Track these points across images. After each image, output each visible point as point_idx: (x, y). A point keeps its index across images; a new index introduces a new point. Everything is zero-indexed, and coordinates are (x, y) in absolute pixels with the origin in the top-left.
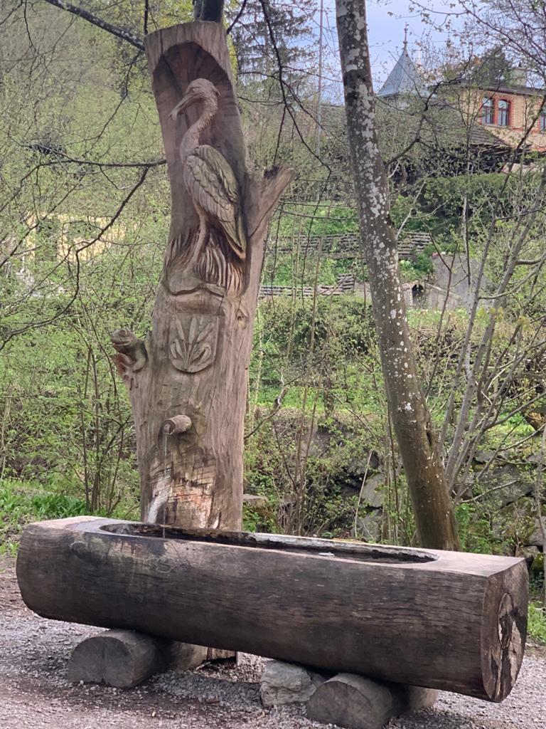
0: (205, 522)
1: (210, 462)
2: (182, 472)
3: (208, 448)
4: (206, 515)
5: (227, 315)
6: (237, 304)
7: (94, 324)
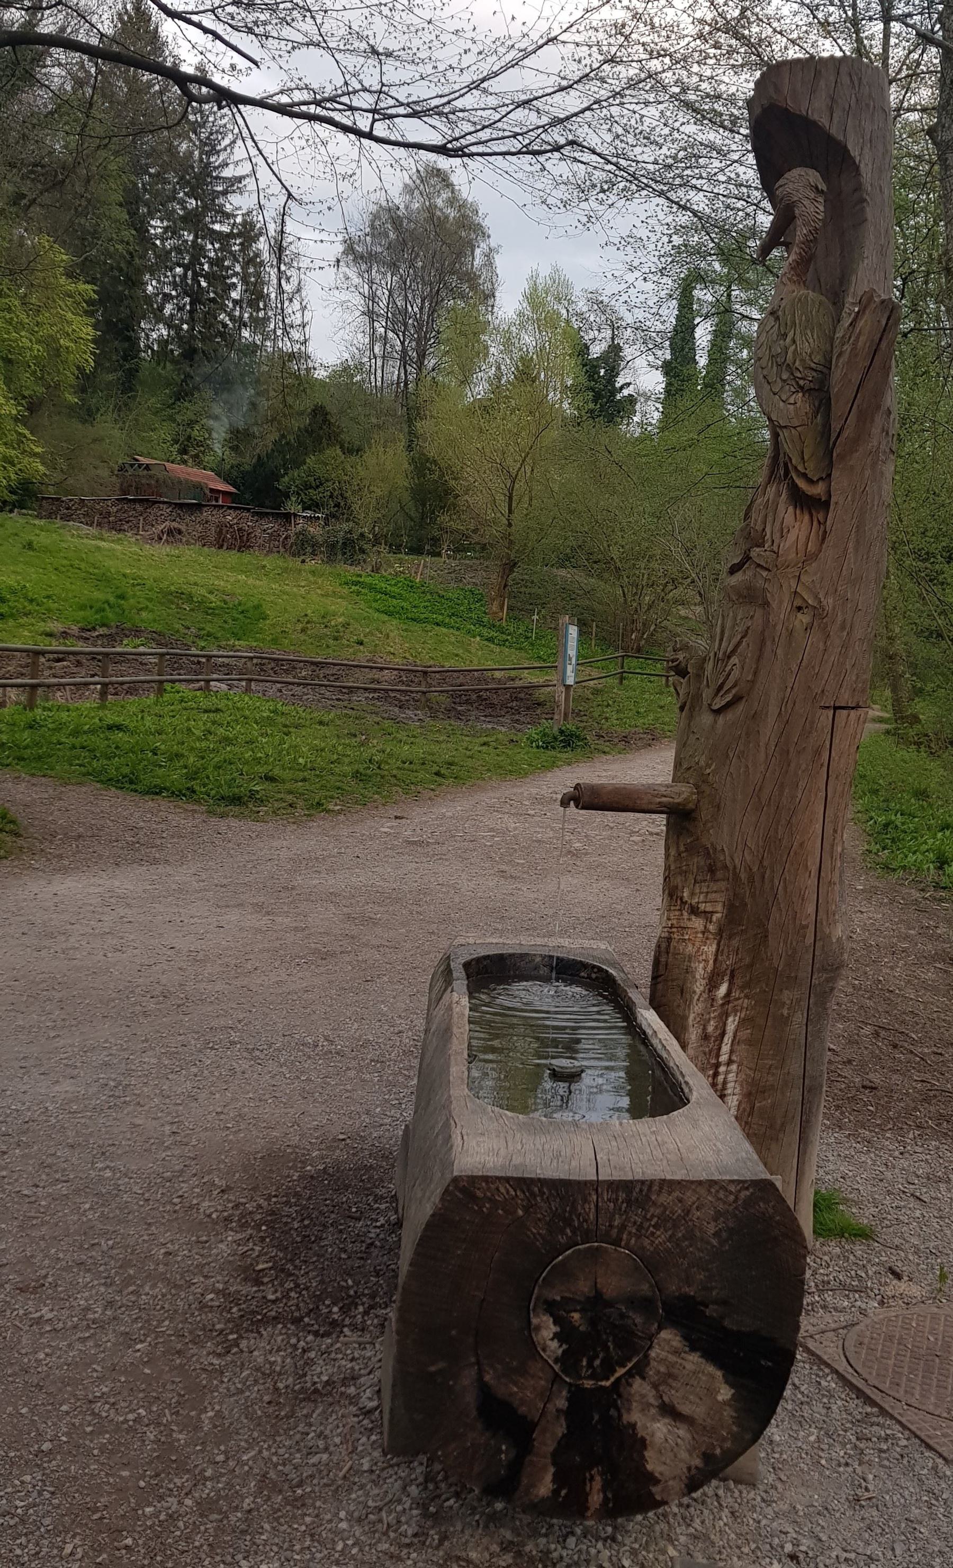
0: (704, 982)
1: (719, 874)
2: (680, 885)
3: (719, 848)
4: (705, 968)
5: (774, 605)
6: (793, 583)
7: (511, 107)
